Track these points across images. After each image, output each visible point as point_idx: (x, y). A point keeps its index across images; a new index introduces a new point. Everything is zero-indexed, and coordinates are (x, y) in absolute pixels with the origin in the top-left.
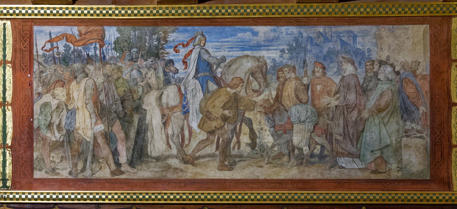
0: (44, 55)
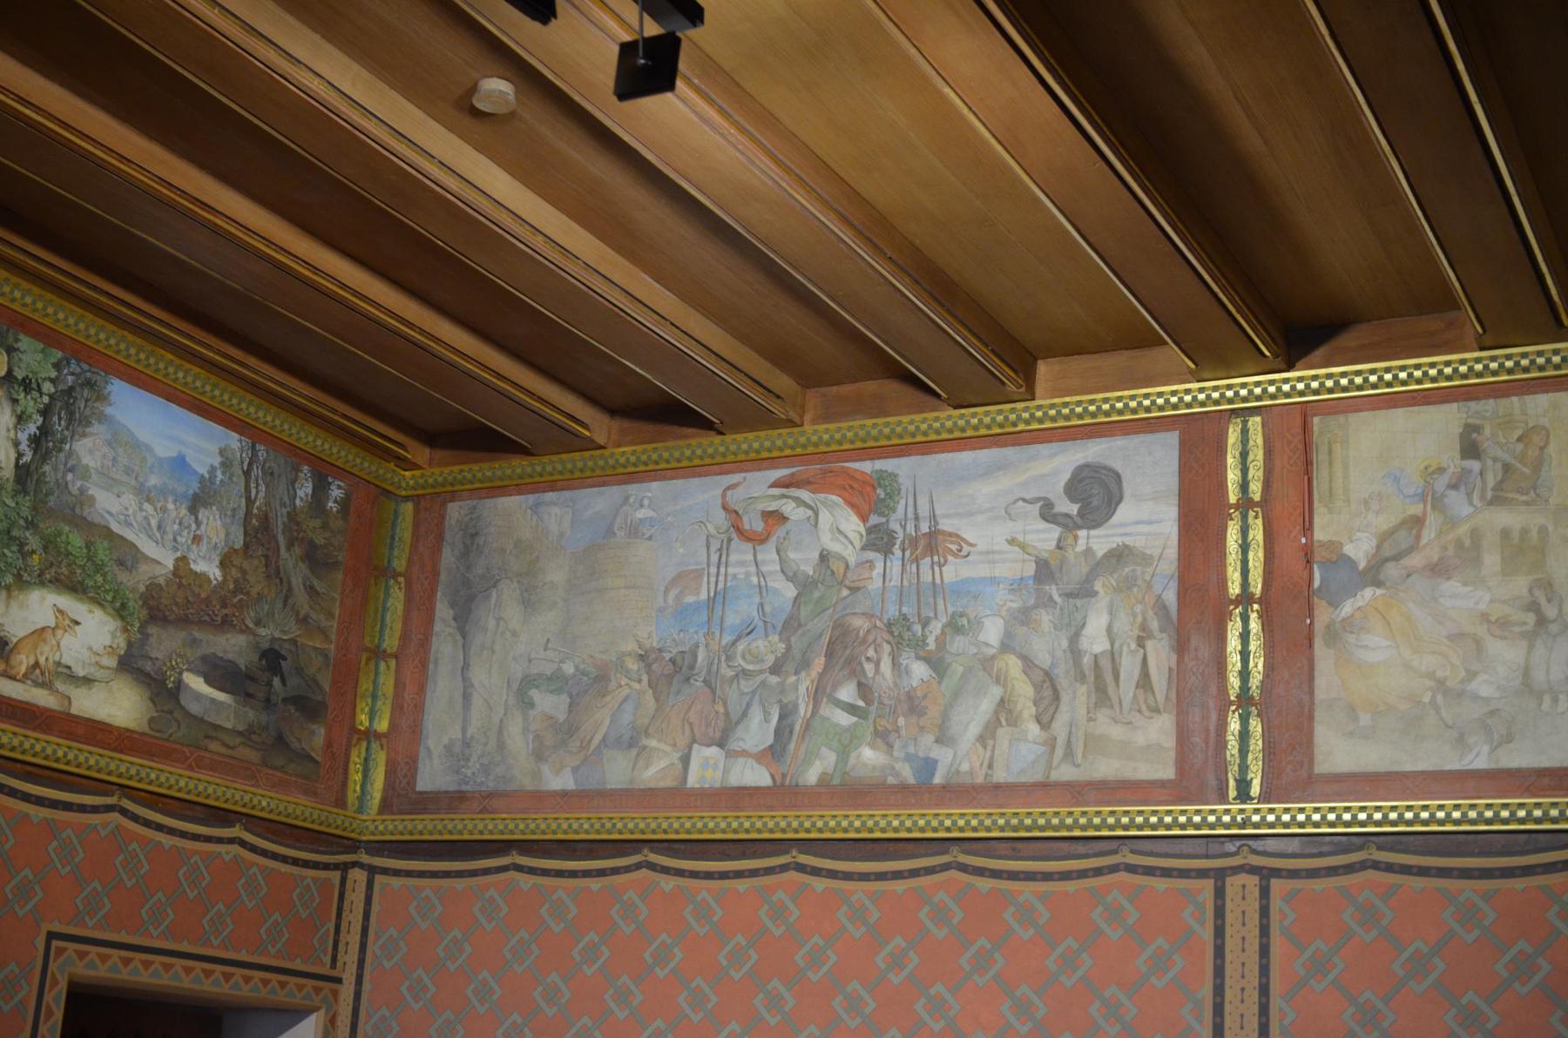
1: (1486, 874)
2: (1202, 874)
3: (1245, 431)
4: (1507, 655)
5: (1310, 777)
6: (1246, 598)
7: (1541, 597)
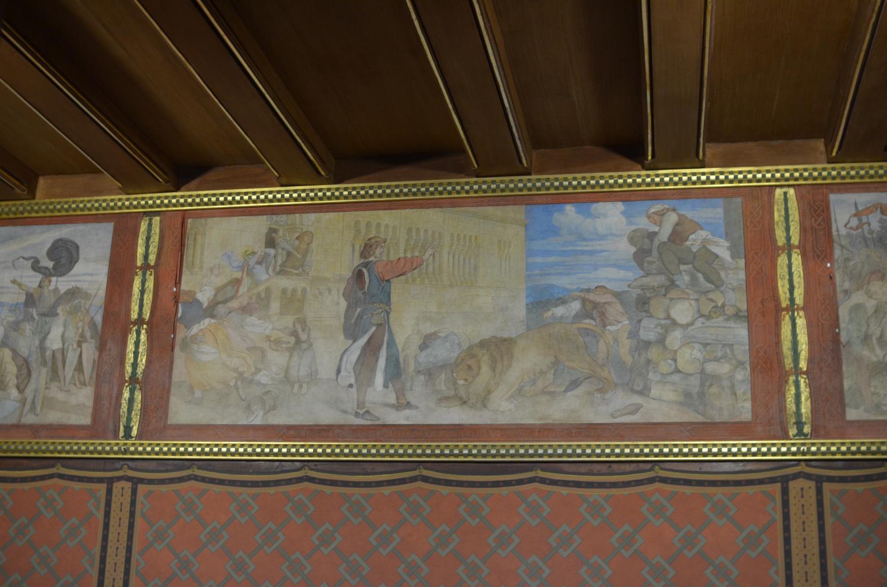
0: (849, 235)
1: (255, 484)
2: (100, 480)
3: (150, 225)
4: (277, 359)
5: (165, 426)
6: (140, 321)
7: (299, 328)
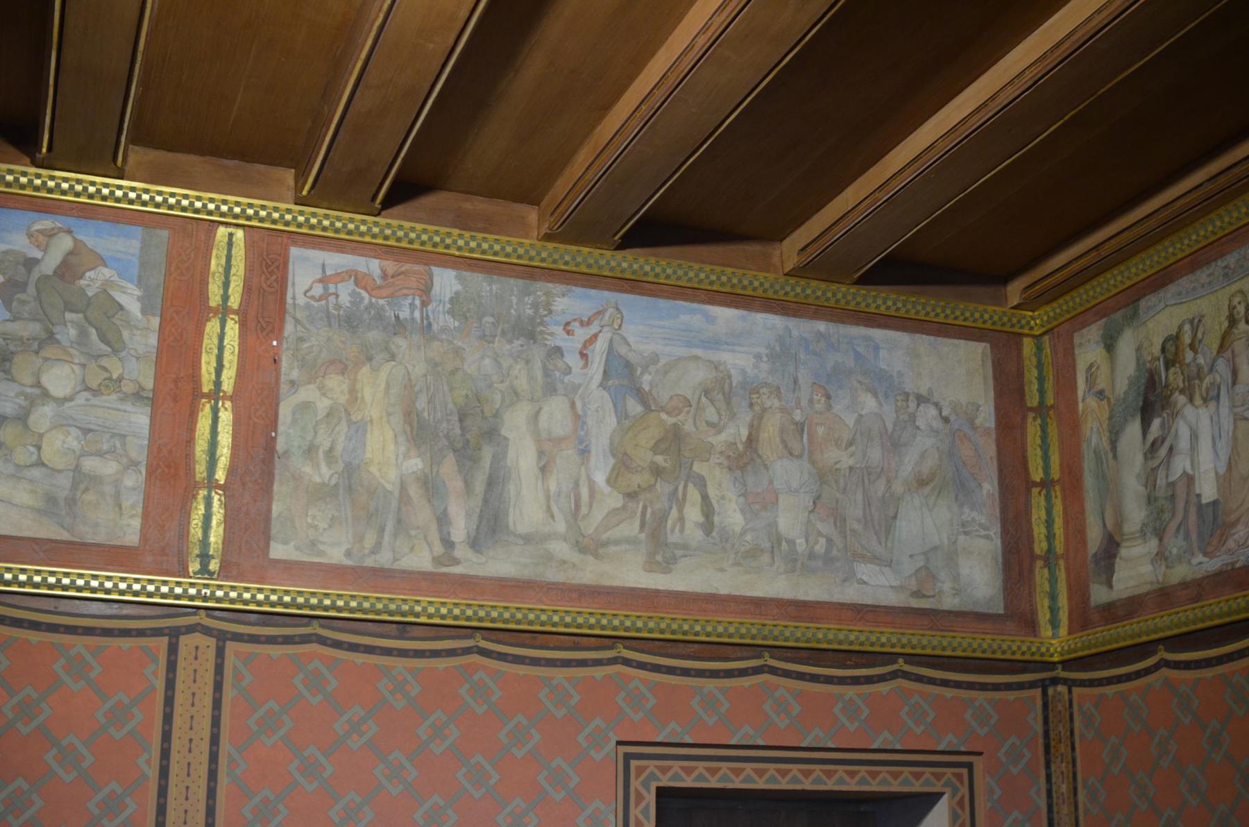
0: (308, 307)
